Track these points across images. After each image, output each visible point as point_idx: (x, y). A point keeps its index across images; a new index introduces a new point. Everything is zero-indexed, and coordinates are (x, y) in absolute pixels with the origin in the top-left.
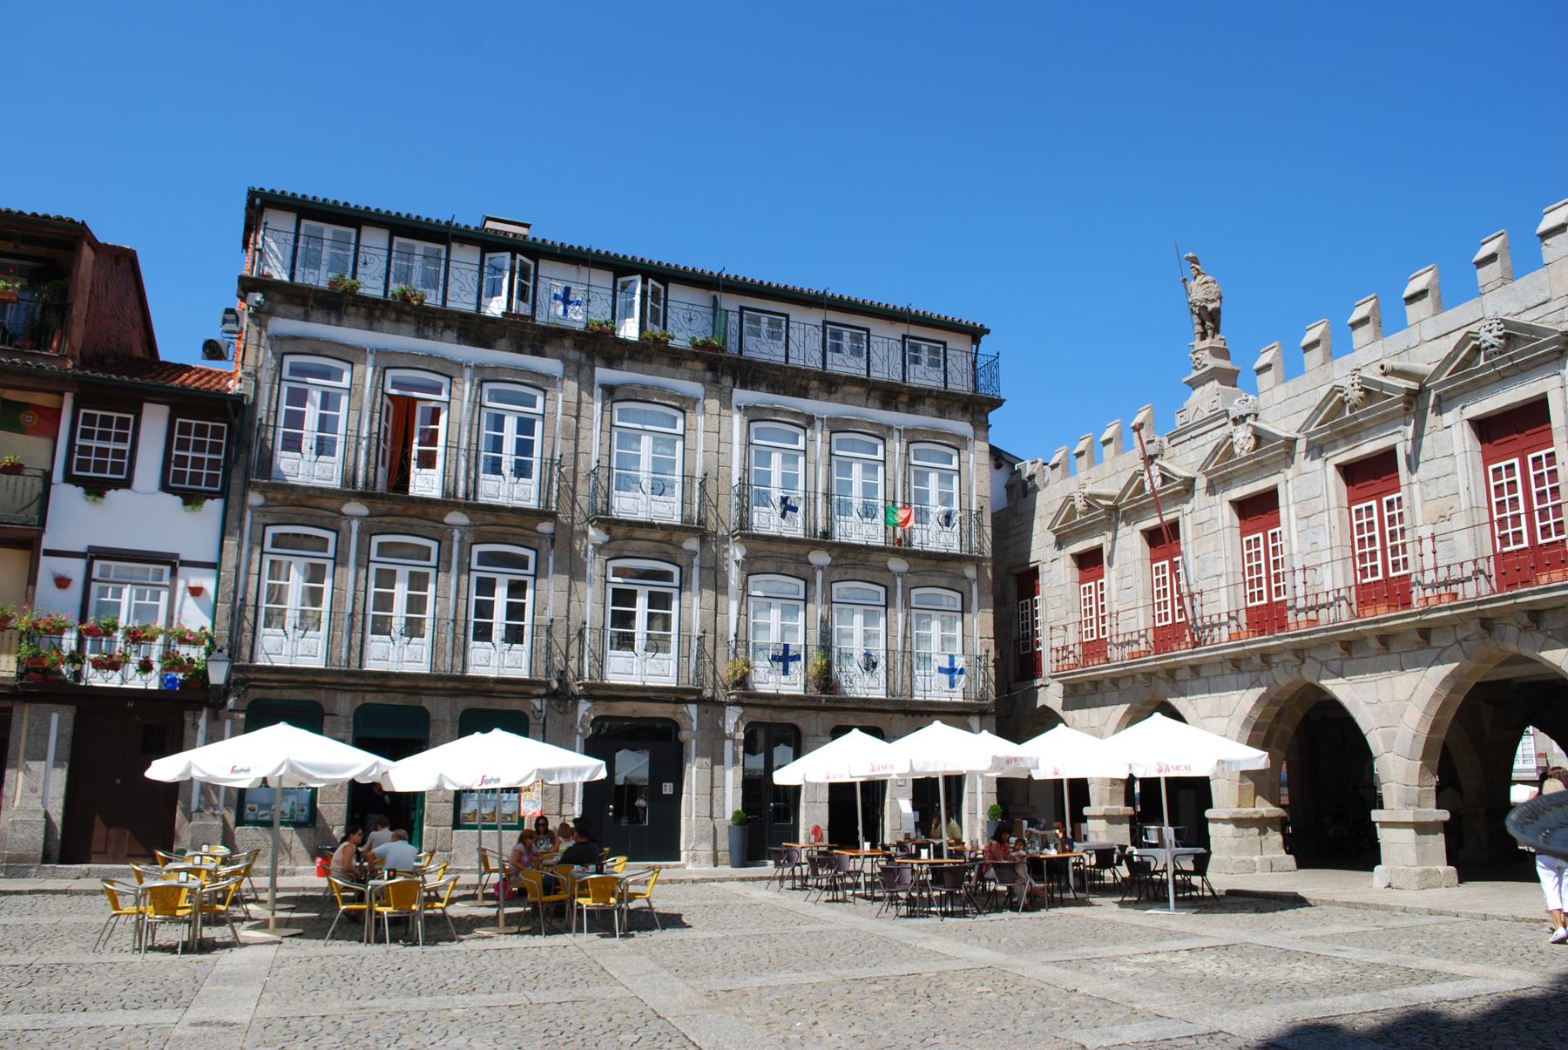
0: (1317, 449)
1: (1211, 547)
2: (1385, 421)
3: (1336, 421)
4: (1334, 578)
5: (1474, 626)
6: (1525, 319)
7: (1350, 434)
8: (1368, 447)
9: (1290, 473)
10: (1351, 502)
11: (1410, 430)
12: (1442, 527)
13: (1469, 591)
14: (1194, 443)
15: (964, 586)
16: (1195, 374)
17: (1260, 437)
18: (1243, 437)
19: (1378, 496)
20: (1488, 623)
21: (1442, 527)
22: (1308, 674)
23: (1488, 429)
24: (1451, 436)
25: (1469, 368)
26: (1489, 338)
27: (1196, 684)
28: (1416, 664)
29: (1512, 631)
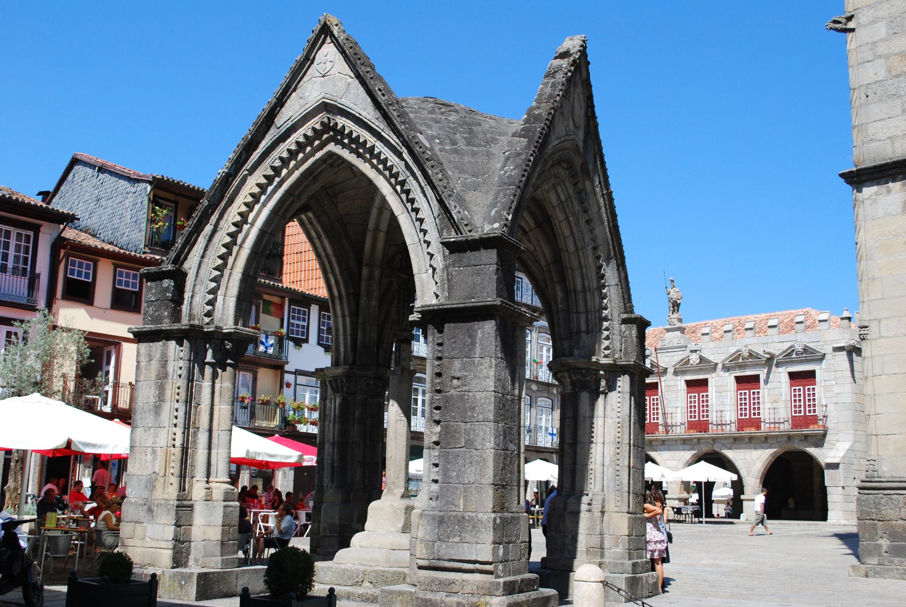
0: (726, 369)
1: (674, 396)
2: (756, 366)
3: (734, 362)
4: (730, 416)
5: (785, 438)
6: (810, 345)
7: (741, 367)
8: (748, 373)
9: (714, 375)
10: (738, 390)
11: (766, 371)
12: (775, 405)
13: (782, 427)
14: (668, 354)
15: (552, 397)
16: (669, 327)
17: (702, 359)
18: (694, 358)
19: (749, 390)
20: (789, 438)
21: (775, 405)
22: (716, 448)
23: (794, 377)
24: (781, 375)
25: (788, 357)
26: (799, 348)
27: (662, 447)
28: (761, 448)
29: (797, 441)
